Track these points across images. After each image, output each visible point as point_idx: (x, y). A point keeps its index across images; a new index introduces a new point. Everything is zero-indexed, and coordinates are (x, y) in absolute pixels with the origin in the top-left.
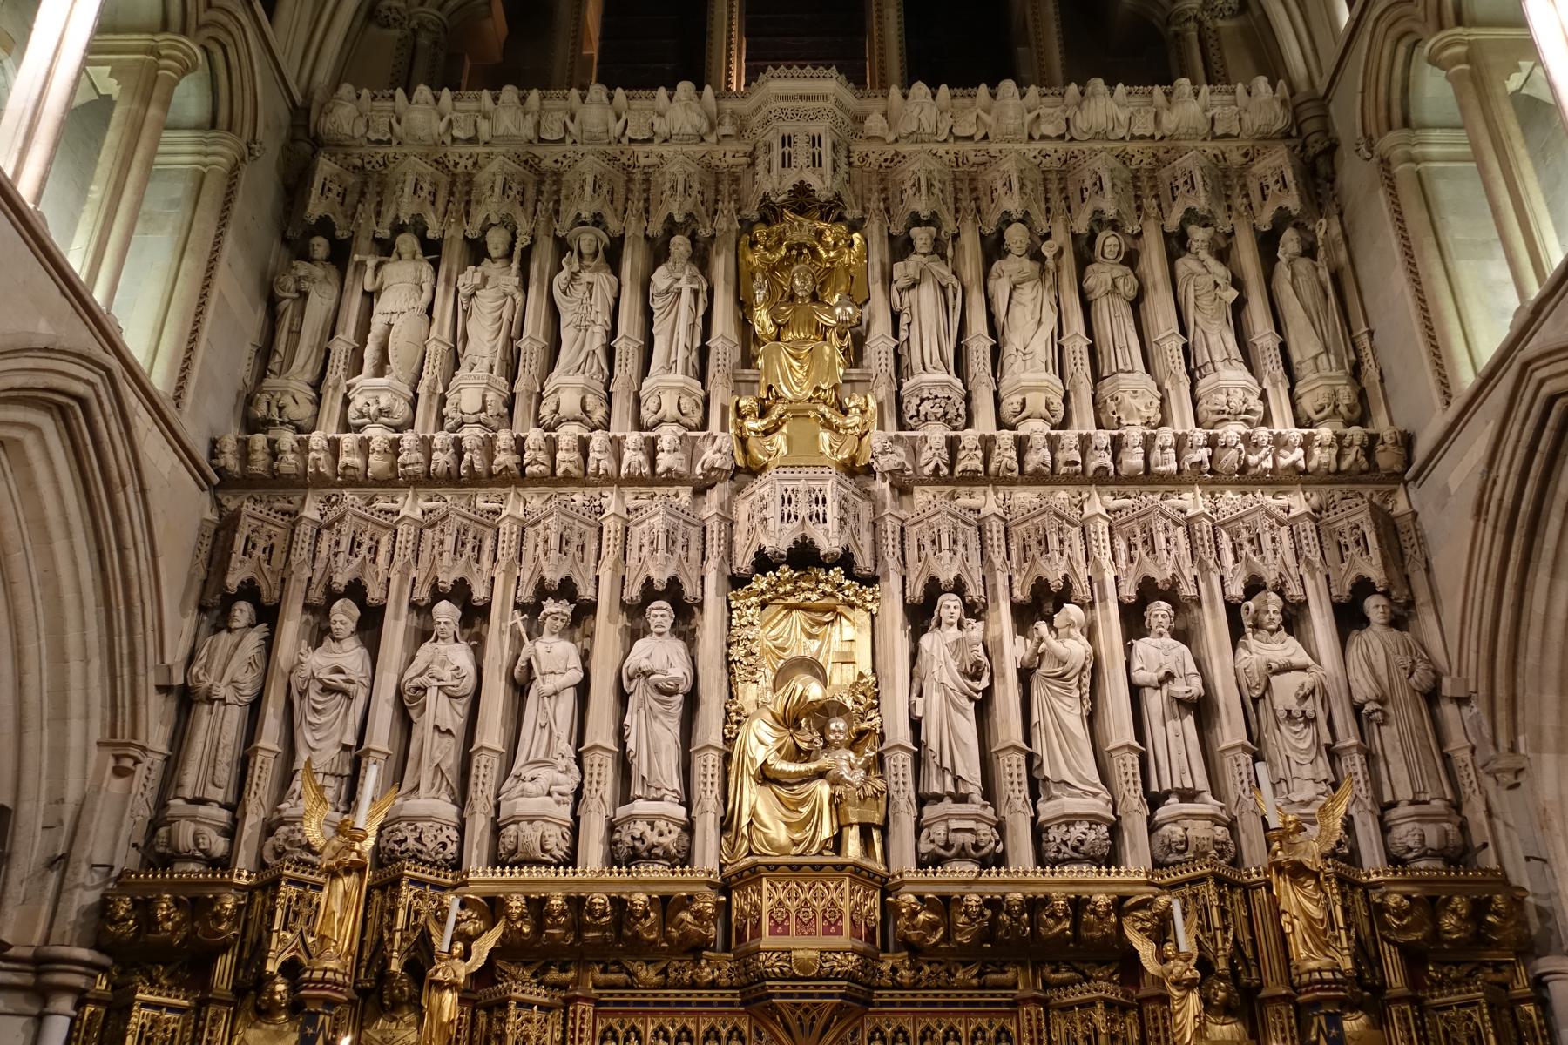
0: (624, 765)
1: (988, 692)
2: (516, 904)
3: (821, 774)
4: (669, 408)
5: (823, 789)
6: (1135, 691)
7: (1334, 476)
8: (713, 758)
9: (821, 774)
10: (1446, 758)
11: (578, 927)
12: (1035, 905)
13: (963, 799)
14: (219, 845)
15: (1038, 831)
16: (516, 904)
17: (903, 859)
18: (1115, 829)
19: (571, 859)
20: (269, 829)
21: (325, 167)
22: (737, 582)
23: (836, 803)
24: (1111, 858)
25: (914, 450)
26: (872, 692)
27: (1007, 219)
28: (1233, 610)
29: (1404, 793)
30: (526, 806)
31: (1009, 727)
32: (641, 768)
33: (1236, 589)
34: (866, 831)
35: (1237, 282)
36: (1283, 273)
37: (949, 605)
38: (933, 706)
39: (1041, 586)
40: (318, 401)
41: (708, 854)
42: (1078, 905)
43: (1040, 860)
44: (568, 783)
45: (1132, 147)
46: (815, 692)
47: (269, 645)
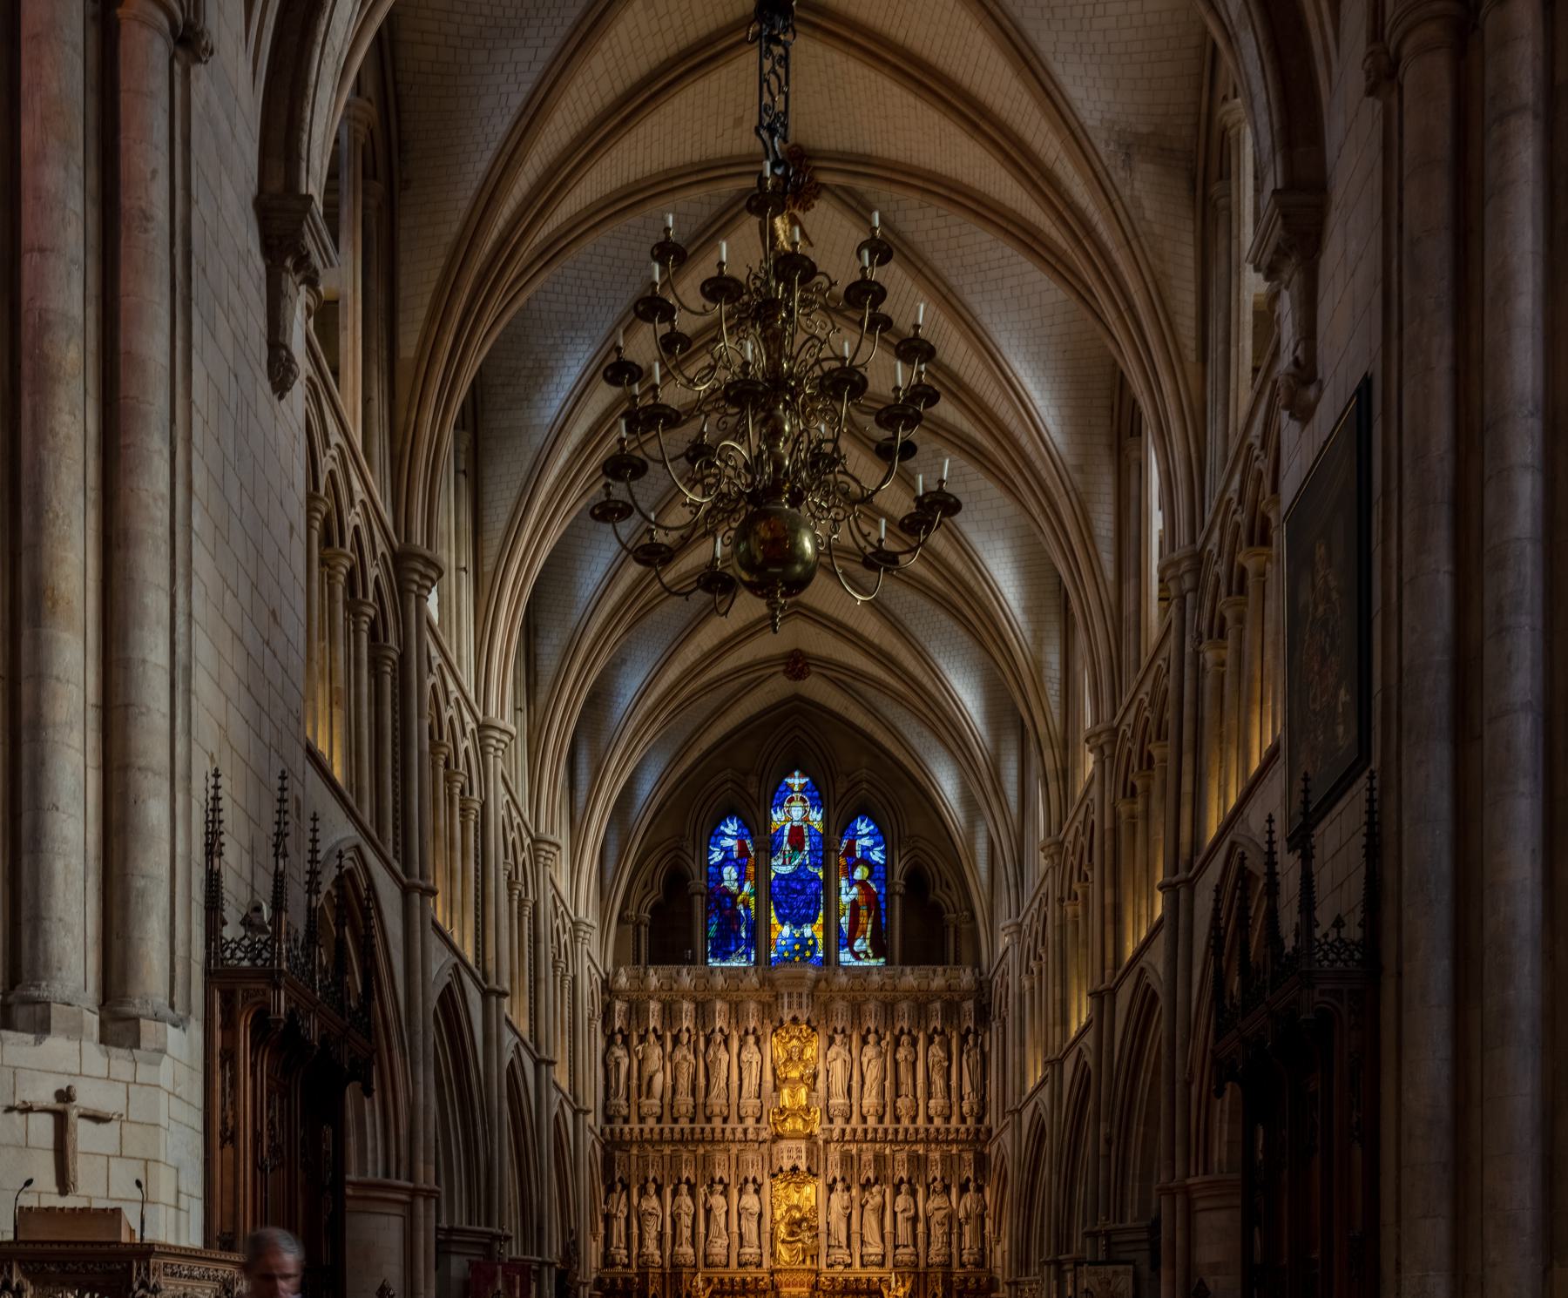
0: (741, 1236)
1: (850, 1213)
2: (716, 1280)
3: (799, 1240)
4: (750, 1112)
5: (800, 1245)
6: (895, 1214)
7: (966, 1141)
8: (768, 1235)
9: (799, 1240)
10: (983, 1236)
11: (733, 1286)
12: (857, 1280)
13: (840, 1247)
14: (626, 1261)
15: (862, 1257)
16: (716, 1280)
17: (823, 1265)
18: (884, 1256)
19: (727, 1265)
20: (639, 1256)
21: (619, 1006)
22: (774, 1176)
23: (804, 1250)
24: (882, 1264)
25: (831, 1131)
26: (815, 1210)
27: (868, 1031)
28: (928, 1186)
29: (968, 1246)
30: (715, 1251)
31: (855, 1226)
32: (746, 1237)
33: (930, 1180)
34: (812, 1256)
35: (950, 1059)
36: (965, 1056)
37: (839, 1186)
38: (833, 1218)
39: (868, 1180)
40: (629, 1107)
41: (767, 1263)
42: (869, 1280)
43: (863, 1265)
44: (726, 1243)
45: (919, 994)
46: (798, 1215)
47: (629, 1198)
